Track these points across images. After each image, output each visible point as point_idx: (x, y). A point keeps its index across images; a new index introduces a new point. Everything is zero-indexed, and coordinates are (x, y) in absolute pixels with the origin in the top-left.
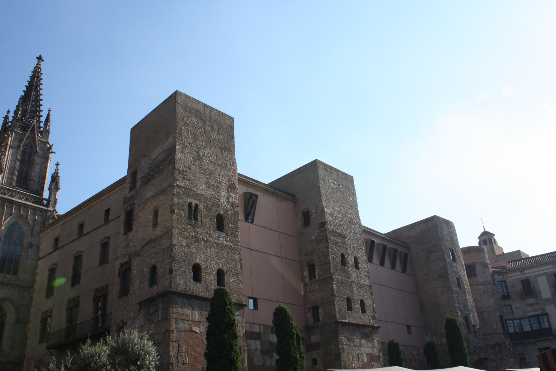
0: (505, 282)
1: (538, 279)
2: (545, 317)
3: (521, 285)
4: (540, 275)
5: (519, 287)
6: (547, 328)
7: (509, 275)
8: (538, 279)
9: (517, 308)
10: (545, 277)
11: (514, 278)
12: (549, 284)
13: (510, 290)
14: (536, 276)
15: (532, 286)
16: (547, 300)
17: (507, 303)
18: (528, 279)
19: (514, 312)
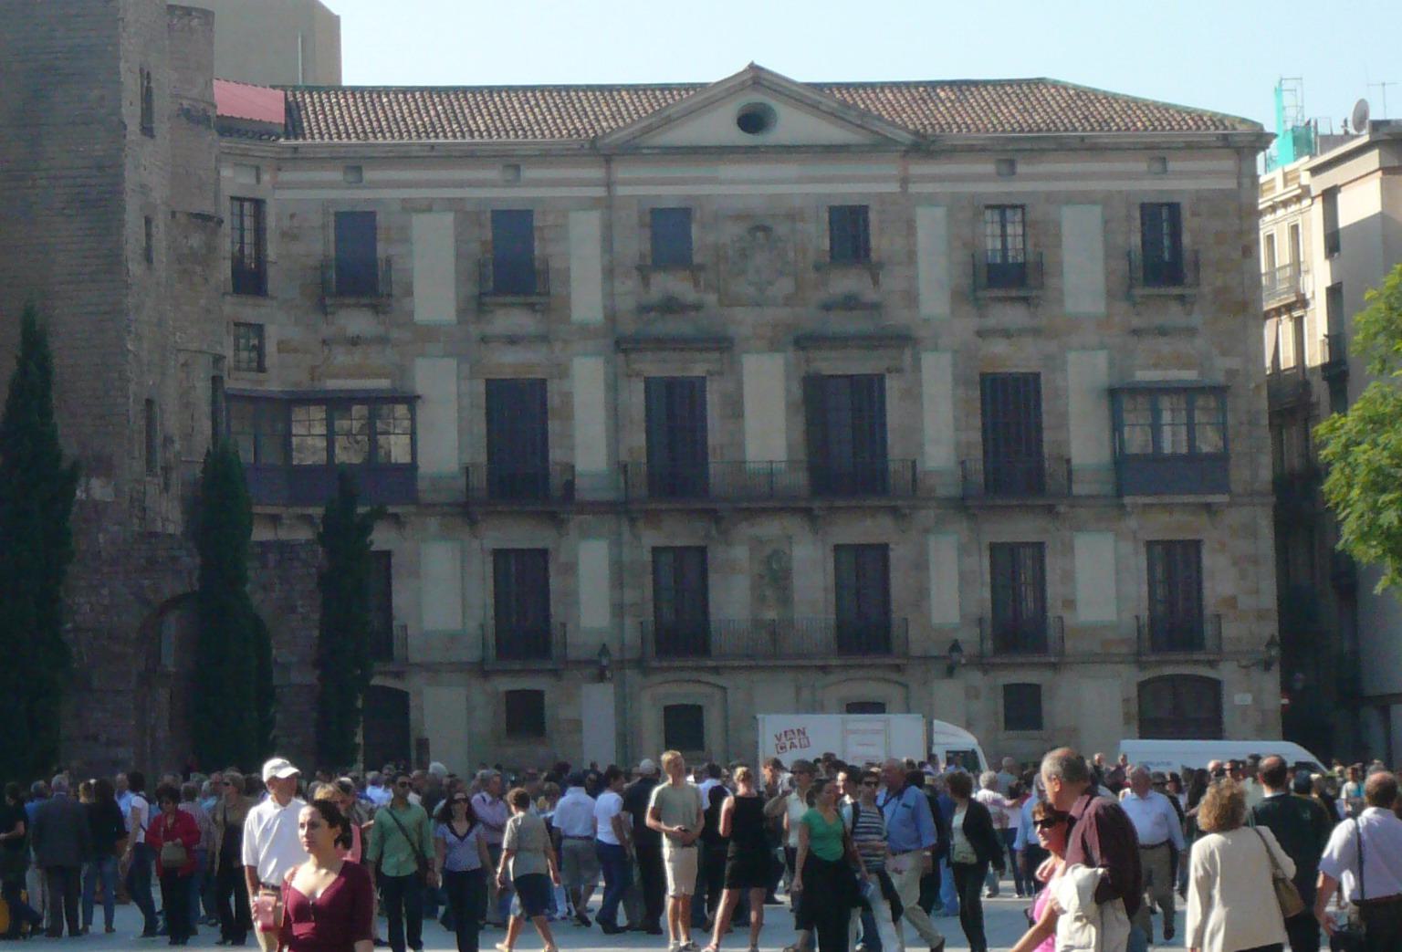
0: (258, 204)
1: (420, 223)
2: (401, 410)
3: (332, 237)
4: (429, 208)
5: (319, 245)
6: (399, 468)
7: (285, 176)
8: (420, 223)
9: (283, 347)
10: (449, 218)
11: (303, 200)
12: (459, 255)
13: (272, 251)
14: (409, 207)
15: (382, 250)
16: (428, 334)
17: (249, 311)
18: (372, 214)
19: (268, 362)
